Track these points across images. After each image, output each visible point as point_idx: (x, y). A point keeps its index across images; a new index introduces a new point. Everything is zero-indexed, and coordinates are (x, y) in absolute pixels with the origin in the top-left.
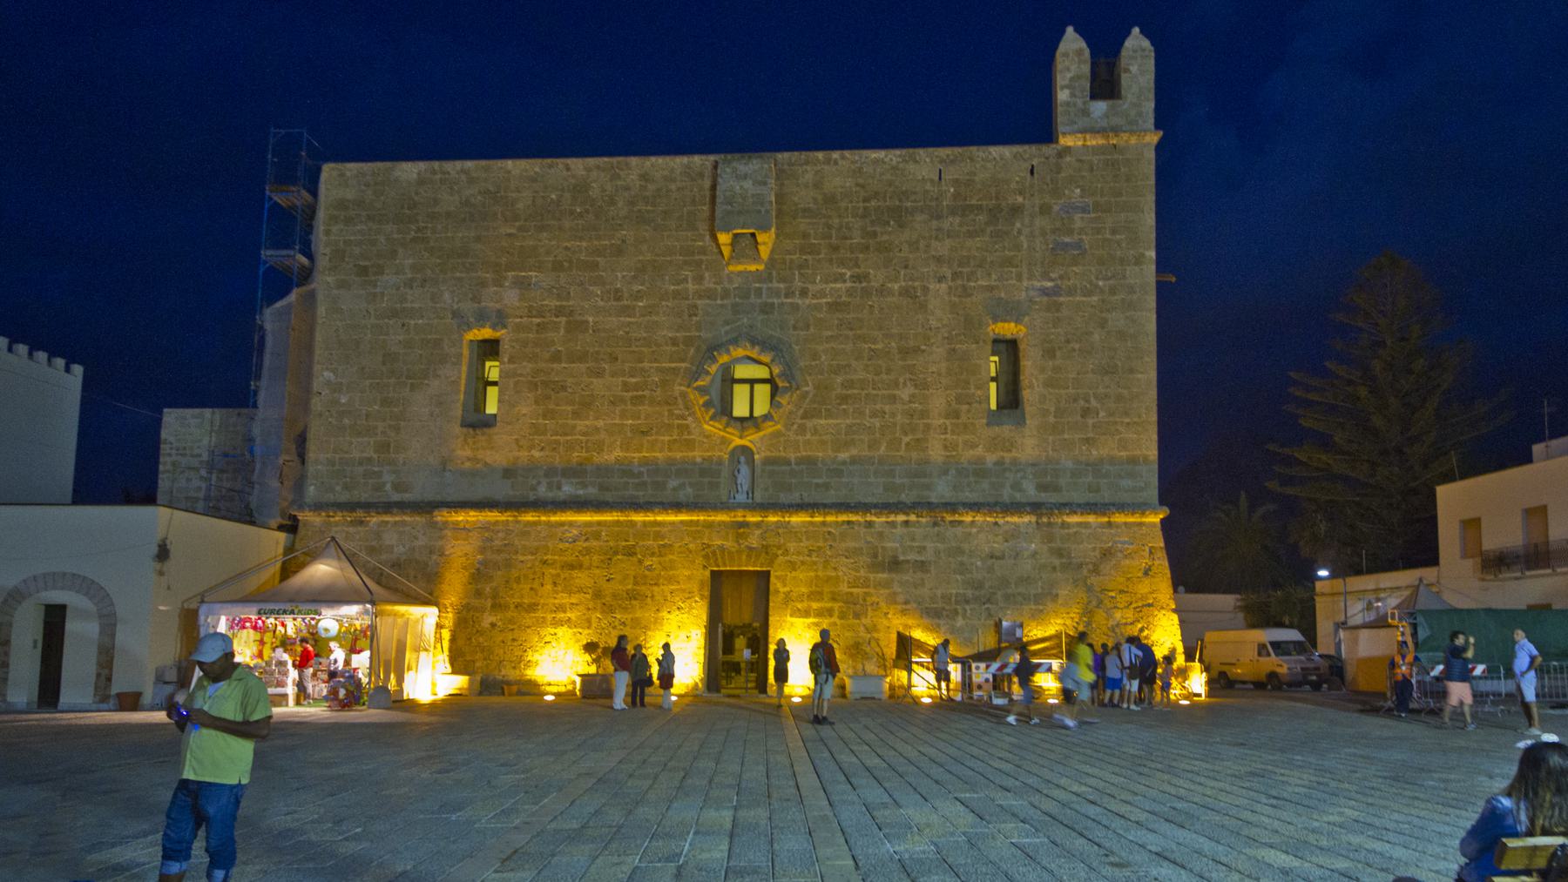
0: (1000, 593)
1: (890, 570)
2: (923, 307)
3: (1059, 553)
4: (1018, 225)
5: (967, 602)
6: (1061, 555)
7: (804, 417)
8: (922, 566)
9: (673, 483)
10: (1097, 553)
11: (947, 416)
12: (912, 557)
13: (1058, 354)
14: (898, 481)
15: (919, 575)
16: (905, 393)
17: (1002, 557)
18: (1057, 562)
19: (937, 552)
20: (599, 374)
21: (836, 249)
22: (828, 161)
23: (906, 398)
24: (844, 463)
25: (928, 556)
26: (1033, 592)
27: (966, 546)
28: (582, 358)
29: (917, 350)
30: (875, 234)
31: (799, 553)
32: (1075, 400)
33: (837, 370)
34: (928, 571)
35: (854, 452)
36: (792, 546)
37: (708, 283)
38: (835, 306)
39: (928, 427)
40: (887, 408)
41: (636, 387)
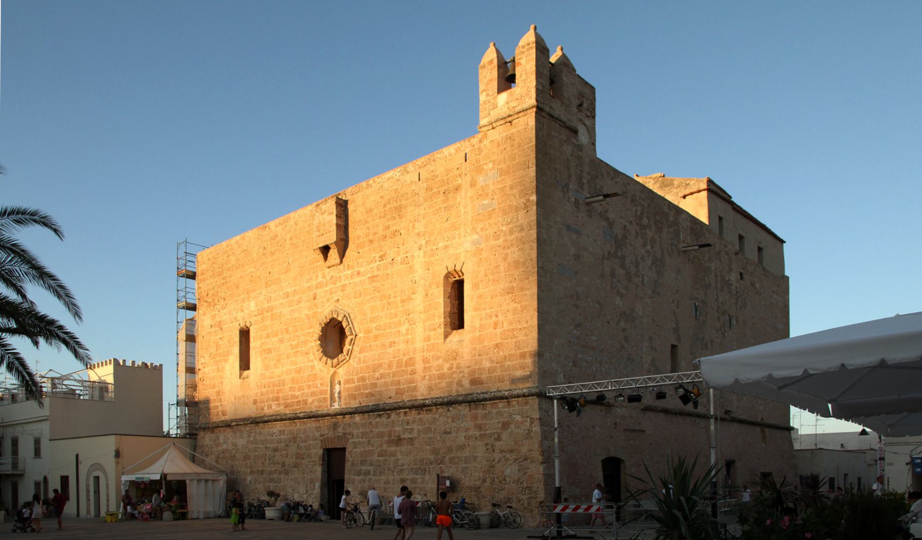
0: (448, 457)
1: (397, 445)
2: (411, 268)
3: (479, 427)
4: (459, 199)
5: (431, 463)
6: (480, 429)
7: (360, 352)
8: (411, 441)
9: (310, 400)
10: (500, 425)
11: (424, 341)
12: (407, 435)
13: (481, 285)
14: (402, 387)
15: (409, 447)
16: (403, 329)
17: (450, 433)
18: (478, 433)
19: (419, 431)
20: (282, 341)
21: (371, 241)
22: (368, 186)
23: (404, 332)
24: (378, 379)
25: (415, 434)
26: (464, 455)
27: (432, 426)
28: (276, 335)
29: (410, 299)
30: (388, 227)
31: (358, 437)
32: (490, 317)
33: (372, 321)
34: (413, 444)
35: (382, 371)
36: (355, 432)
37: (320, 279)
38: (373, 278)
39: (415, 349)
40: (396, 340)
41: (297, 346)
